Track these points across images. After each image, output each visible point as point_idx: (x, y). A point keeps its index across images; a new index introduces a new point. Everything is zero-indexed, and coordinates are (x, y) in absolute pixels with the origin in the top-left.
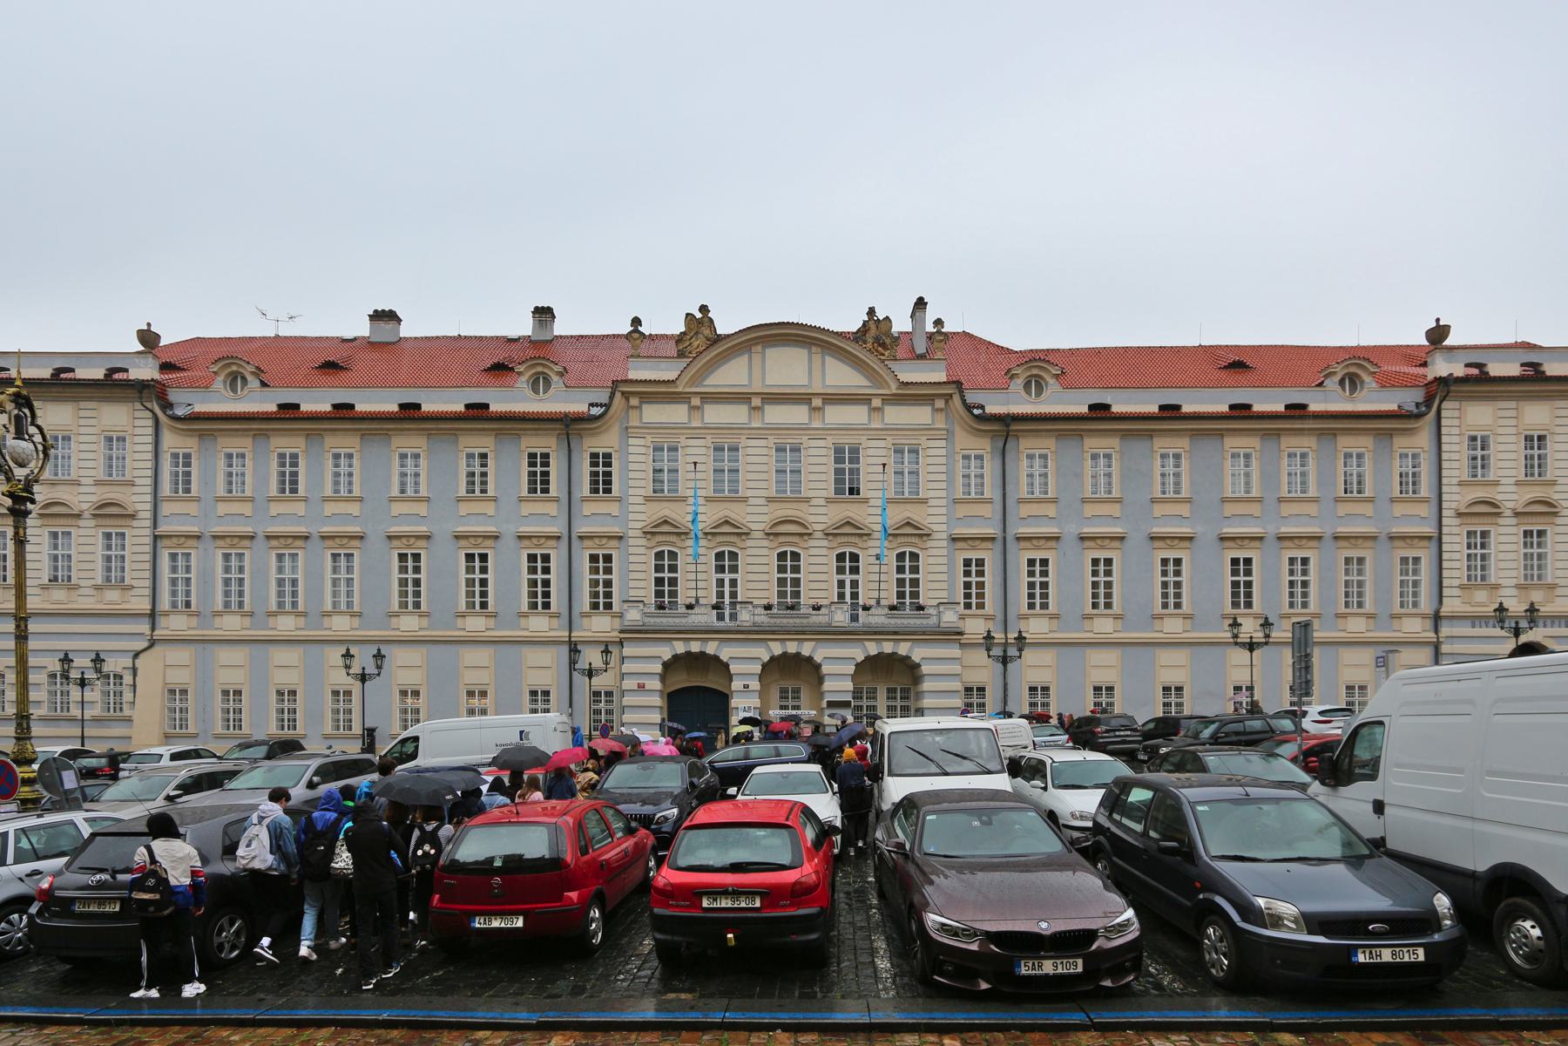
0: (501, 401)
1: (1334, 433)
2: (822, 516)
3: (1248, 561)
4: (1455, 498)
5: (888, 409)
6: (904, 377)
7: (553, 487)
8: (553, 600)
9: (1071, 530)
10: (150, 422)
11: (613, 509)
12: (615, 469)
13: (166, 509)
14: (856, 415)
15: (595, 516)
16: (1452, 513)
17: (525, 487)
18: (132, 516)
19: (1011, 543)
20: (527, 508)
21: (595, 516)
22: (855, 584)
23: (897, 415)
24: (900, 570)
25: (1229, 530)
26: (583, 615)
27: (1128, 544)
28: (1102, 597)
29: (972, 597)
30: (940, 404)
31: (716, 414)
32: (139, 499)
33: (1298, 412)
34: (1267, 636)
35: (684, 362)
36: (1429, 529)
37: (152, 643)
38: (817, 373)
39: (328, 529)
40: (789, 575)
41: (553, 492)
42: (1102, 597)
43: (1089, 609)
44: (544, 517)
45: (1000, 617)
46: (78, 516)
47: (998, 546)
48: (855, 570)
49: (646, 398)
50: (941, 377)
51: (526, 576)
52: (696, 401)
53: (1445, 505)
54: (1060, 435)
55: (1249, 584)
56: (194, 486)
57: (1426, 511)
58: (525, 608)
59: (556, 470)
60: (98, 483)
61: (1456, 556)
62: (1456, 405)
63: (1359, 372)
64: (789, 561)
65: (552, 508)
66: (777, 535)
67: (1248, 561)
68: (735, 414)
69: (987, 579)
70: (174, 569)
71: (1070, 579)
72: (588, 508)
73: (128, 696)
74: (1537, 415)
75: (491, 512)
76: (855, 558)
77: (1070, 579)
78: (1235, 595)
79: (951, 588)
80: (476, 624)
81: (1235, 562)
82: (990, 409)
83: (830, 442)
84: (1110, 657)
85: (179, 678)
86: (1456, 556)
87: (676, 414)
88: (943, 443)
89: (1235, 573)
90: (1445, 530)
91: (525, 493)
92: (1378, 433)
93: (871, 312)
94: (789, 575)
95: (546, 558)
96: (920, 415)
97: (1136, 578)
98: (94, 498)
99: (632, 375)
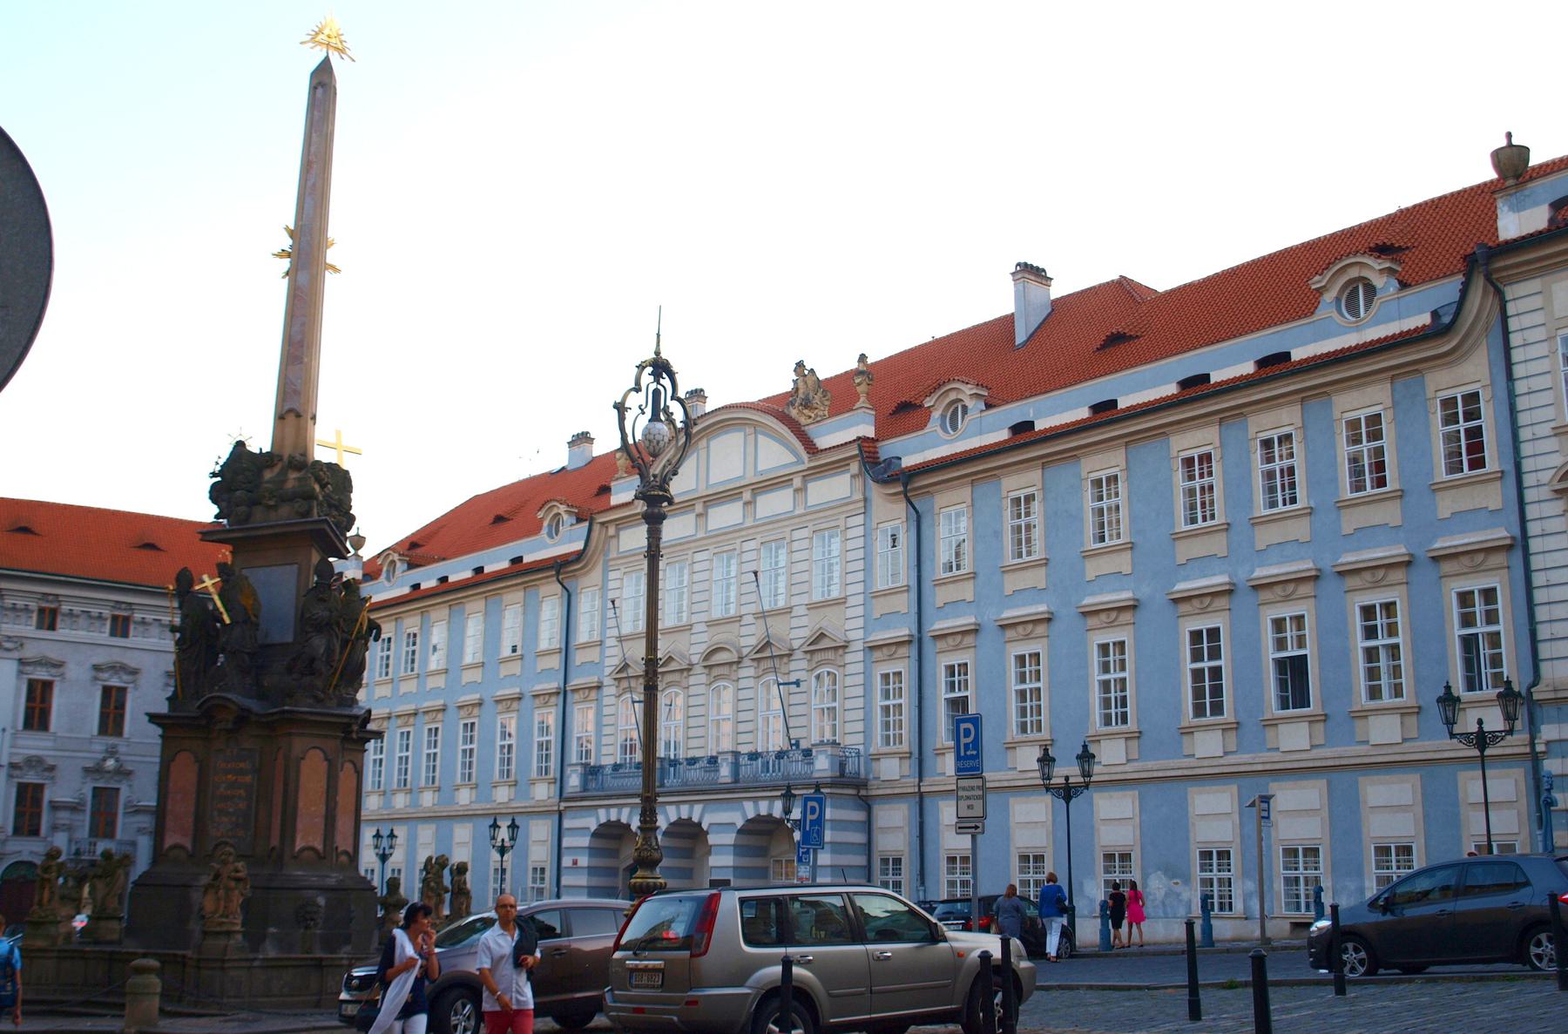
1: (1323, 391)
3: (1214, 634)
5: (813, 487)
16: (1545, 493)
19: (929, 647)
27: (1057, 626)
33: (1277, 369)
47: (915, 646)
53: (1528, 480)
54: (974, 480)
55: (1216, 673)
57: (1494, 497)
62: (1534, 285)
66: (710, 667)
67: (1214, 634)
75: (518, 671)
78: (1198, 693)
81: (1196, 636)
88: (860, 519)
89: (1197, 656)
90: (1533, 529)
92: (1394, 374)
93: (800, 365)
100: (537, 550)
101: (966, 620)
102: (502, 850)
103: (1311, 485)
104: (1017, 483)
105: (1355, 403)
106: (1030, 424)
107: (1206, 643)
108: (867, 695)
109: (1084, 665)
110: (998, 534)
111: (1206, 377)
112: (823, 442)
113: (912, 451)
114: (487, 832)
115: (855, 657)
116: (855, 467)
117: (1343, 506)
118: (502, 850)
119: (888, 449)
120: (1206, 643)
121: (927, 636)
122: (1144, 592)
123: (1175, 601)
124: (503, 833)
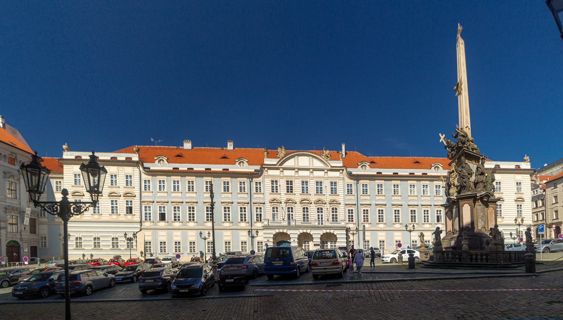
0: (232, 168)
2: (313, 198)
3: (414, 211)
5: (329, 172)
6: (332, 165)
7: (246, 190)
8: (247, 219)
9: (373, 203)
10: (138, 172)
11: (262, 196)
12: (262, 186)
13: (143, 194)
14: (321, 174)
15: (257, 198)
17: (239, 190)
18: (135, 196)
20: (240, 196)
21: (257, 198)
22: (322, 215)
23: (331, 174)
24: (333, 212)
25: (410, 203)
26: (255, 223)
28: (381, 219)
29: (351, 219)
30: (341, 171)
31: (286, 173)
32: (136, 192)
35: (278, 160)
37: (141, 230)
38: (311, 163)
39: (187, 200)
40: (306, 213)
41: (246, 192)
42: (381, 219)
43: (378, 222)
44: (245, 198)
45: (357, 224)
46: (120, 196)
48: (322, 212)
49: (269, 169)
50: (341, 165)
51: (240, 213)
52: (281, 169)
55: (415, 216)
56: (151, 189)
58: (239, 221)
59: (247, 186)
60: (124, 187)
64: (305, 210)
65: (246, 196)
67: (414, 211)
68: (292, 173)
69: (354, 214)
70: (146, 210)
71: (373, 216)
72: (255, 196)
73: (134, 244)
76: (322, 209)
77: (373, 216)
78: (412, 219)
79: (345, 217)
80: (227, 225)
81: (411, 211)
82: (353, 173)
83: (314, 180)
84: (383, 233)
85: (148, 239)
87: (277, 172)
89: (412, 213)
91: (239, 192)
94: (306, 213)
95: (245, 208)
96: (337, 174)
97: (388, 215)
98: (124, 192)
99: (265, 163)
103: (430, 192)
104: (378, 182)
105: (436, 183)
106: (381, 173)
107: (413, 212)
108: (345, 212)
110: (375, 189)
113: (355, 172)
117: (434, 196)
120: (413, 212)
121: (359, 205)
122: (403, 203)
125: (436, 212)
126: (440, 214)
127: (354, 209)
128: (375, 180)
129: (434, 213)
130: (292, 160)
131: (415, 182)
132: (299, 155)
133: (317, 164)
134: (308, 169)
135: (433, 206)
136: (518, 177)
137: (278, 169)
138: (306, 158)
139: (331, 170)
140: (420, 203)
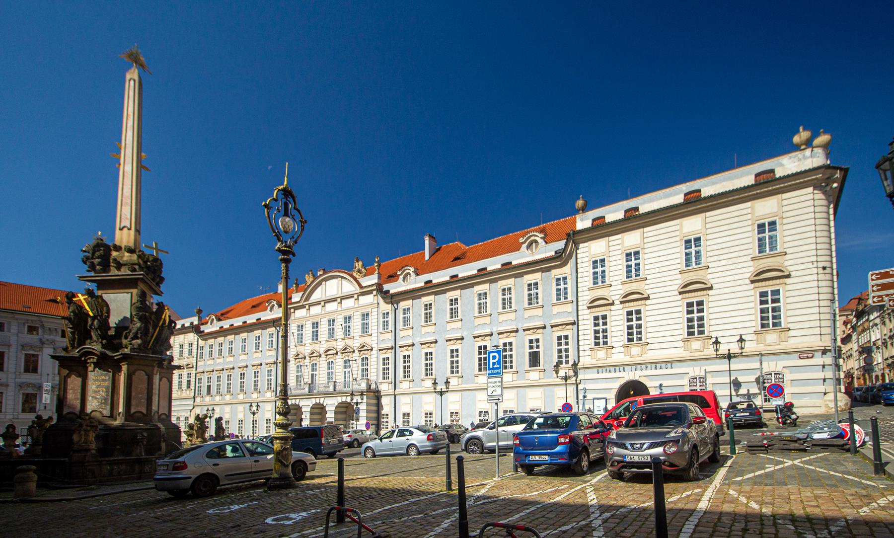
4: (585, 297)
9: (418, 340)
25: (477, 332)
31: (315, 310)
34: (447, 388)
36: (571, 319)
57: (570, 308)
61: (588, 332)
63: (532, 238)
74: (631, 239)
86: (588, 332)
100: (266, 316)
101: (410, 342)
102: (254, 414)
106: (431, 281)
109: (446, 356)
110: (420, 315)
111: (486, 269)
112: (364, 284)
113: (393, 288)
114: (248, 408)
115: (374, 352)
116: (375, 293)
118: (254, 414)
119: (386, 287)
122: (465, 334)
123: (475, 337)
124: (254, 408)
125: (527, 344)
126: (538, 347)
127: (390, 355)
128: (420, 297)
129: (524, 347)
130: (319, 289)
131: (487, 286)
132: (326, 280)
133: (349, 287)
134: (334, 300)
135: (521, 331)
136: (766, 208)
137: (303, 307)
138: (335, 281)
139: (363, 294)
140: (495, 330)
